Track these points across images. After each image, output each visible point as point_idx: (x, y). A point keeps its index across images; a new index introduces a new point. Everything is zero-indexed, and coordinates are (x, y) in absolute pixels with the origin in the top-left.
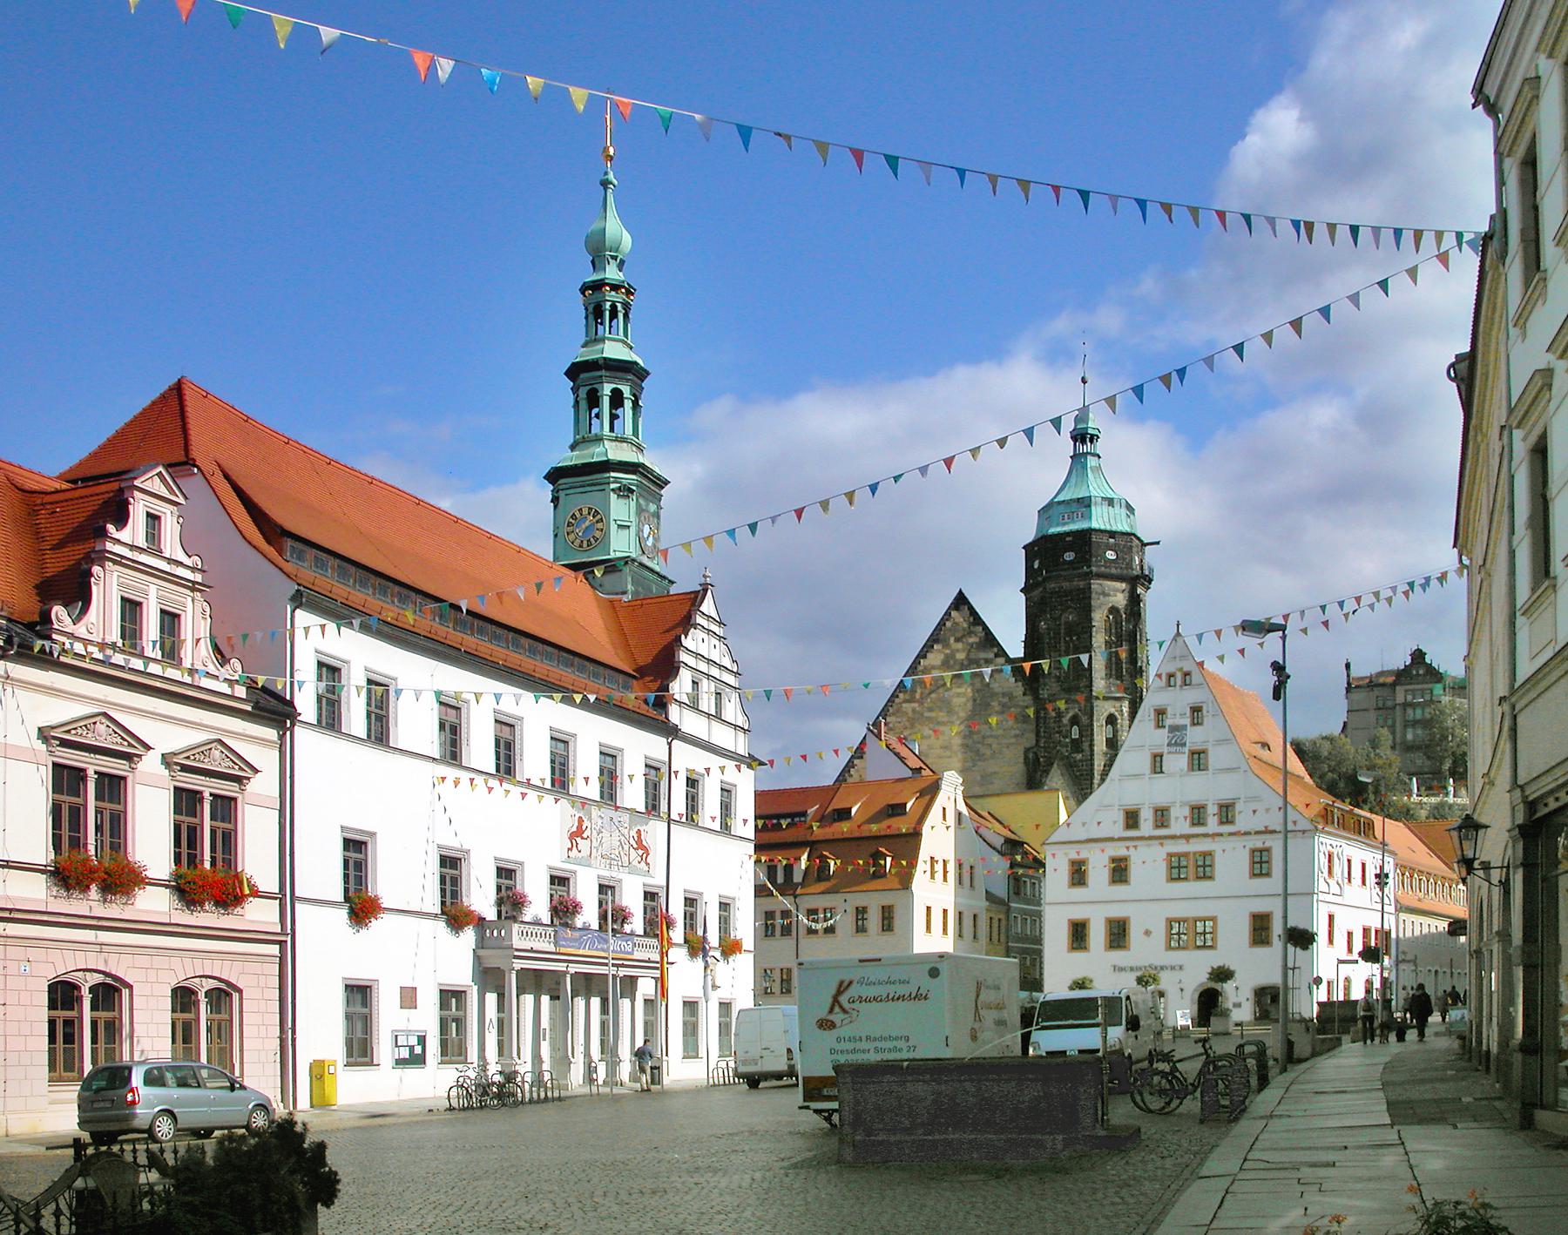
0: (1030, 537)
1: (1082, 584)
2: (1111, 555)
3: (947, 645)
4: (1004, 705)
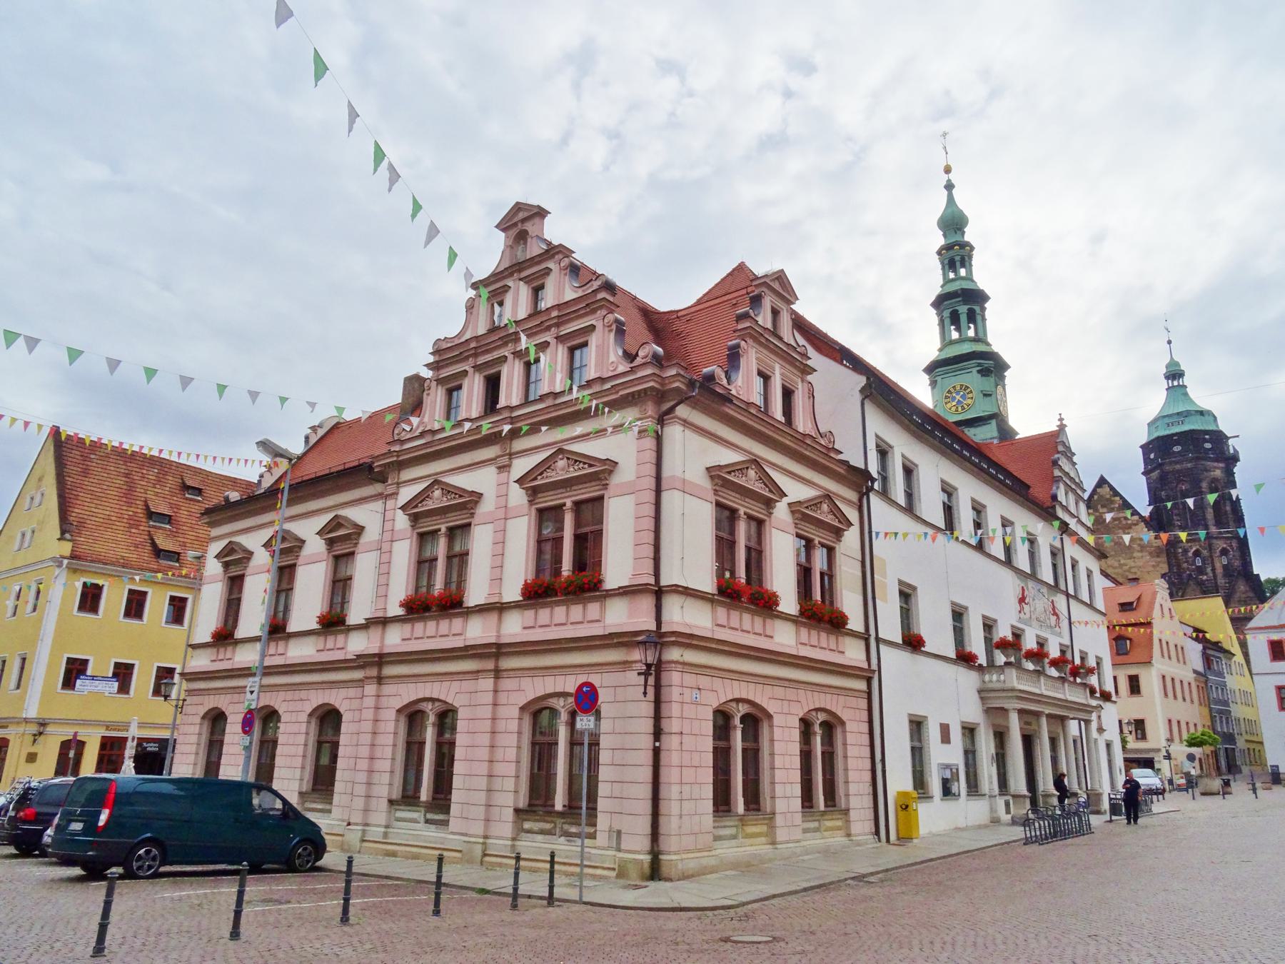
0: (1144, 440)
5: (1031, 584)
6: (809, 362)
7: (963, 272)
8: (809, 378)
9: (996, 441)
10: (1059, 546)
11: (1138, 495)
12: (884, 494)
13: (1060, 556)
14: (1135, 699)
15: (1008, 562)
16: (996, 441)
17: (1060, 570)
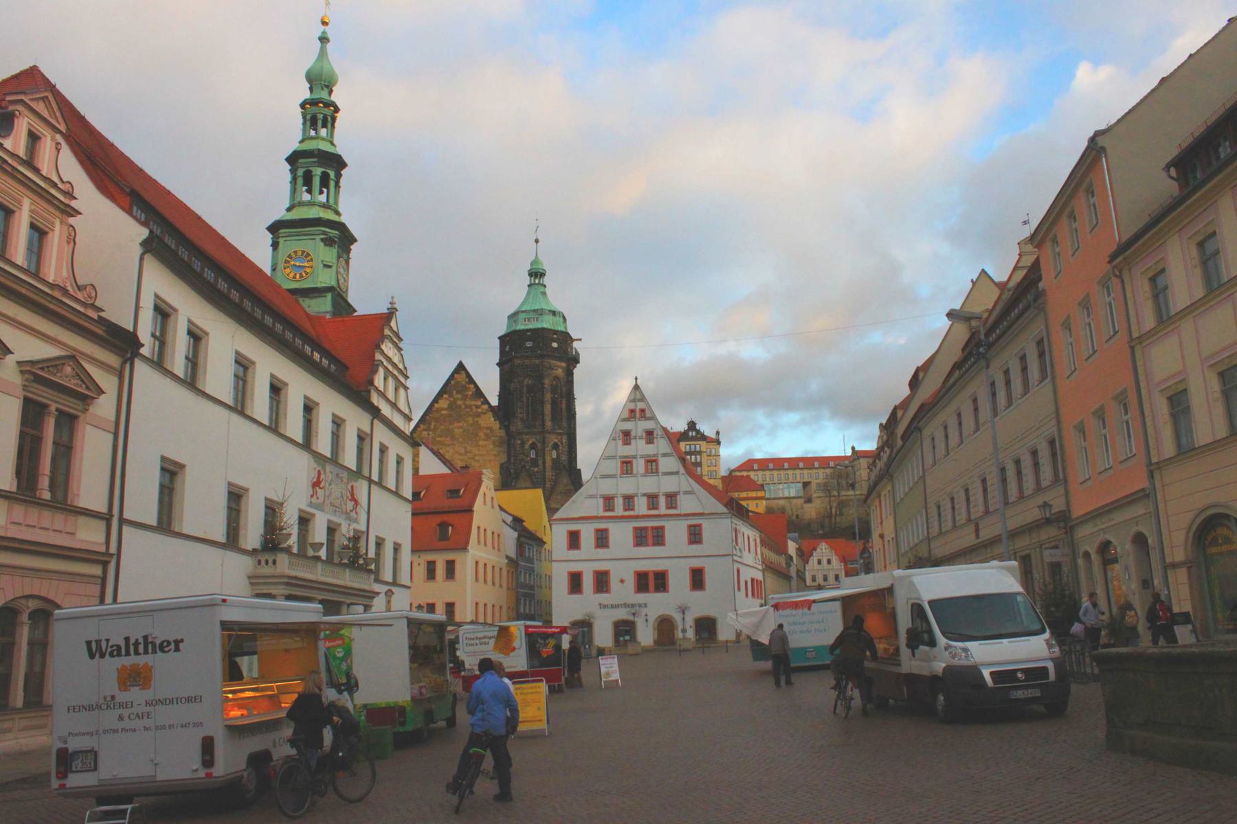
0: (502, 333)
1: (537, 362)
2: (555, 345)
3: (451, 396)
4: (486, 435)
5: (329, 468)
6: (73, 204)
7: (323, 132)
8: (71, 220)
9: (328, 316)
10: (368, 430)
11: (489, 382)
12: (159, 364)
13: (367, 441)
14: (450, 584)
15: (307, 445)
16: (328, 316)
17: (366, 455)
